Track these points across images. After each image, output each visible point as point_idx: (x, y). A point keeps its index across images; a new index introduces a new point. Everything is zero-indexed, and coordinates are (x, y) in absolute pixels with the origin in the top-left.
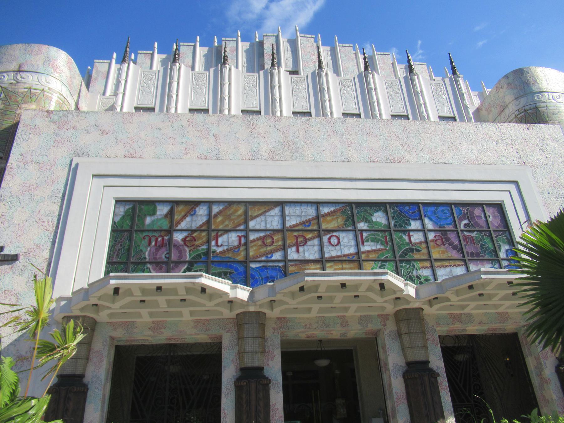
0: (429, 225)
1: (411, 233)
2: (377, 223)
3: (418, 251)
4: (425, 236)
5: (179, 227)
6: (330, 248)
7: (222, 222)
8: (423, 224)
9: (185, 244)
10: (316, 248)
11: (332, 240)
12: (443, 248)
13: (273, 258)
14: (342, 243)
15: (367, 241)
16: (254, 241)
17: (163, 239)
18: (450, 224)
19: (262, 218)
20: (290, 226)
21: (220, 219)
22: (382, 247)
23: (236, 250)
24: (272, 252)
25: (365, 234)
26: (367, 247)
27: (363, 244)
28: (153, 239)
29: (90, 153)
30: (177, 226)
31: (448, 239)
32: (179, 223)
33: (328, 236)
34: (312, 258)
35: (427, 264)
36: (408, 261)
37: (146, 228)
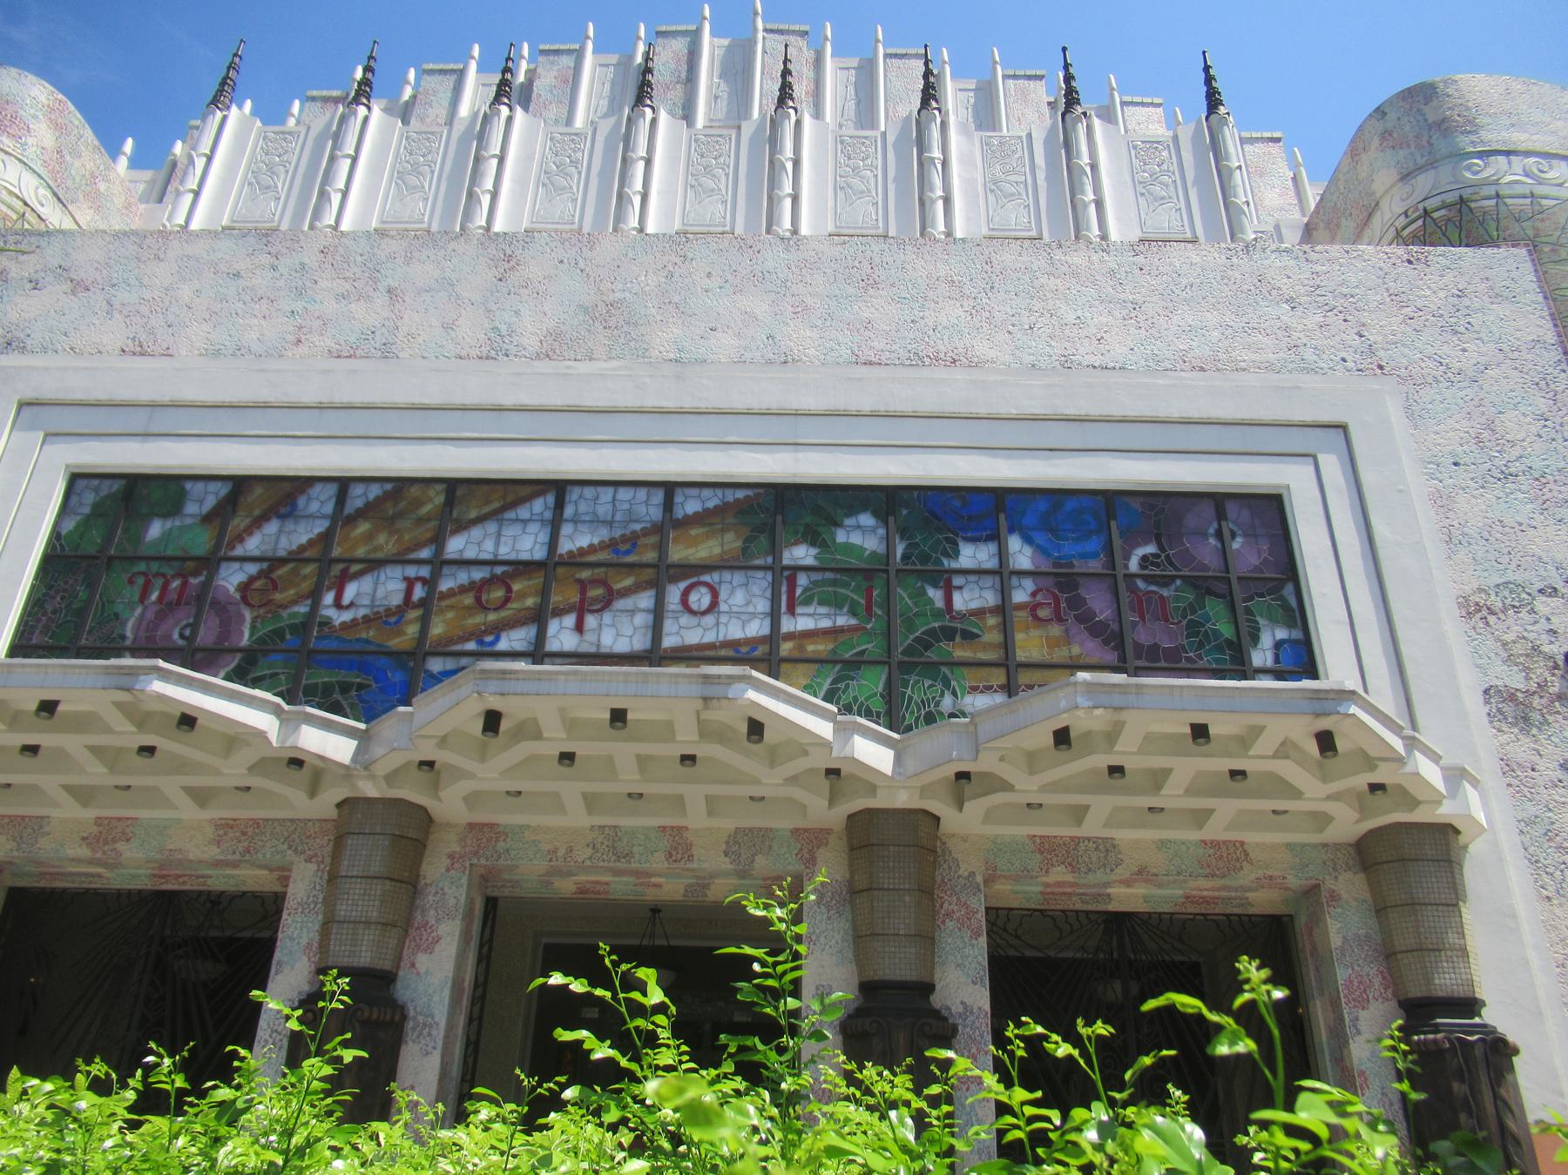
0: (1021, 555)
1: (957, 581)
2: (849, 548)
3: (969, 636)
4: (1004, 592)
5: (239, 551)
6: (685, 619)
7: (369, 537)
8: (1002, 554)
9: (244, 599)
10: (642, 620)
11: (693, 598)
12: (1055, 630)
13: (503, 645)
14: (723, 607)
15: (807, 601)
16: (451, 593)
17: (185, 584)
18: (1095, 555)
19: (491, 527)
20: (570, 553)
21: (363, 527)
22: (853, 622)
23: (393, 619)
24: (498, 629)
25: (802, 580)
26: (802, 622)
27: (791, 611)
28: (159, 582)
29: (29, 342)
30: (233, 548)
31: (1076, 603)
32: (240, 538)
33: (683, 585)
34: (622, 646)
35: (999, 677)
36: (932, 669)
37: (144, 551)
